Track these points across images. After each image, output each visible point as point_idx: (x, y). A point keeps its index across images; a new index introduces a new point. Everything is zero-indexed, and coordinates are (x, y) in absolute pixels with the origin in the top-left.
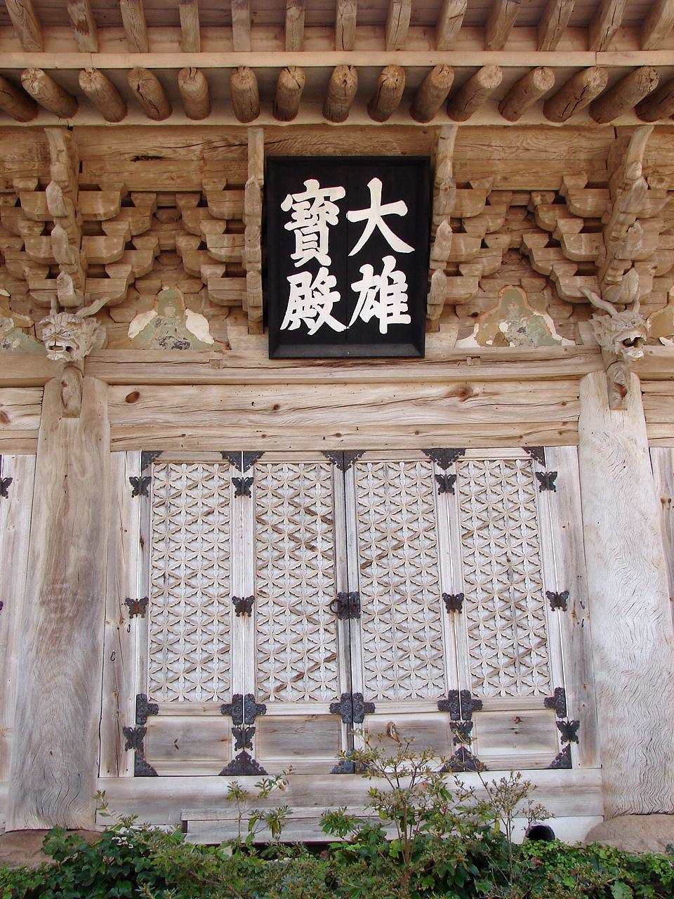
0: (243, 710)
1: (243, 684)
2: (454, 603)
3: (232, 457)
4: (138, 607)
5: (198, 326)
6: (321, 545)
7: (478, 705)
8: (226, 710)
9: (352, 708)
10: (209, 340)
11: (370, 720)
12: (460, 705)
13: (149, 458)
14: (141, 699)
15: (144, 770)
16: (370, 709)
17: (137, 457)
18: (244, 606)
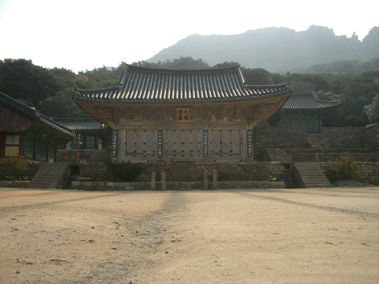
0: (174, 151)
1: (174, 149)
2: (191, 143)
3: (173, 130)
4: (166, 143)
5: (171, 119)
6: (181, 138)
7: (193, 151)
8: (173, 151)
9: (183, 151)
10: (172, 120)
11: (184, 152)
12: (191, 151)
13: (167, 130)
14: (167, 150)
15: (167, 156)
16: (184, 151)
17: (166, 130)
18: (174, 143)
